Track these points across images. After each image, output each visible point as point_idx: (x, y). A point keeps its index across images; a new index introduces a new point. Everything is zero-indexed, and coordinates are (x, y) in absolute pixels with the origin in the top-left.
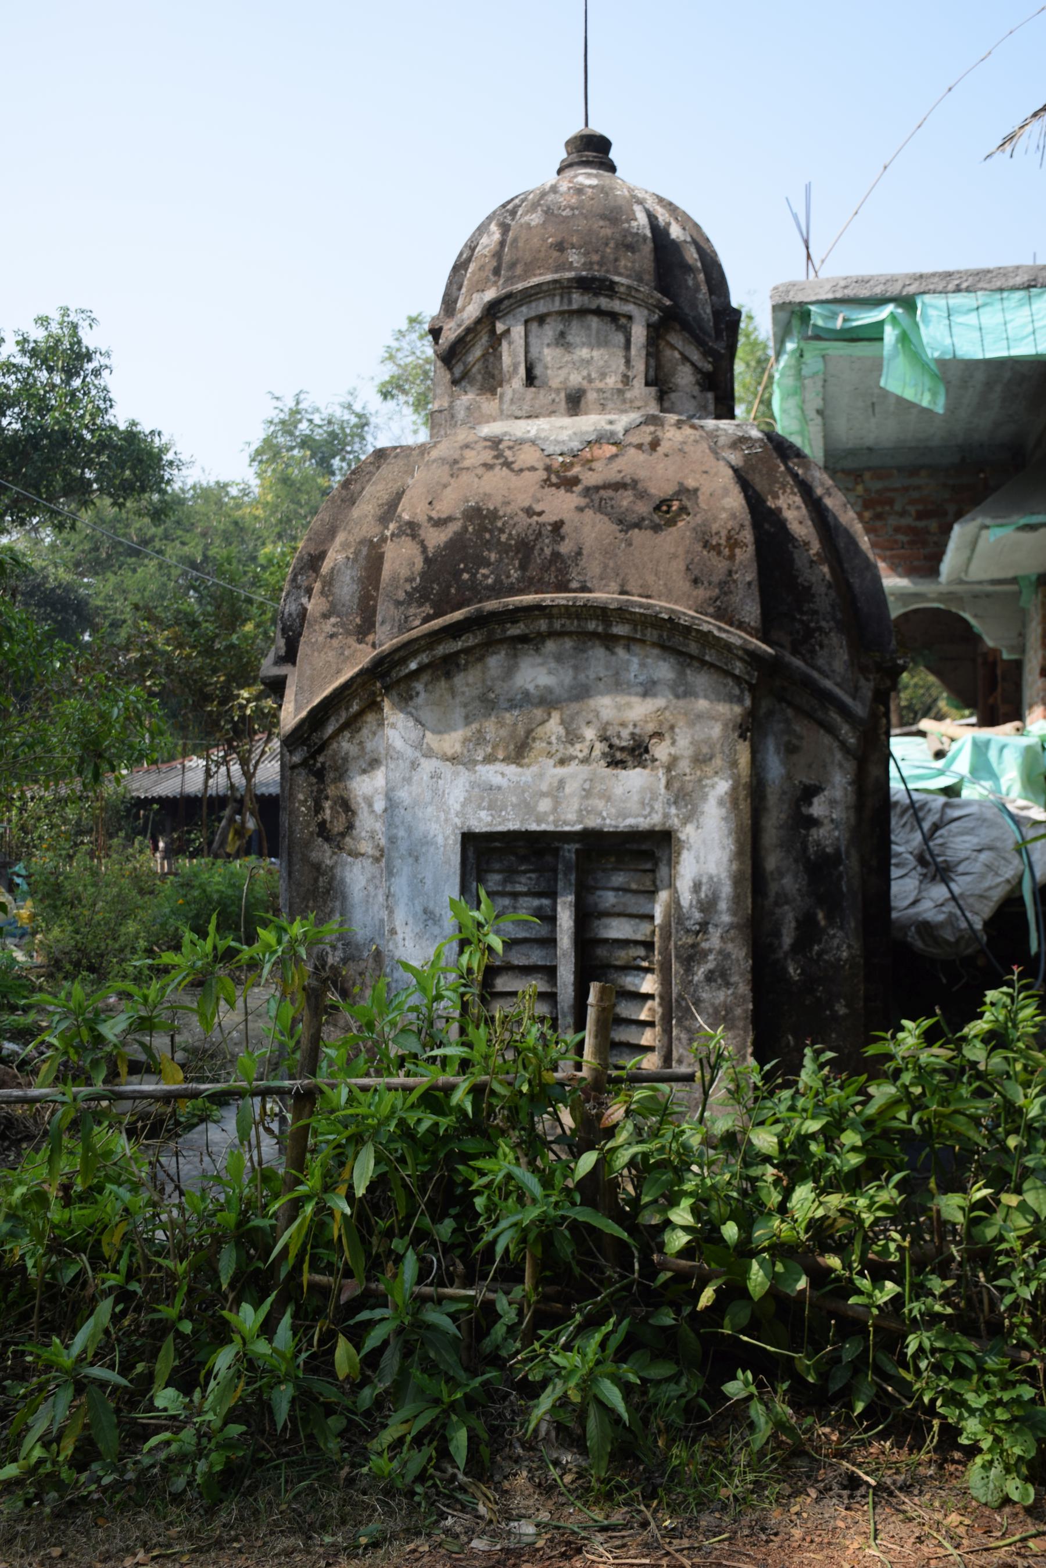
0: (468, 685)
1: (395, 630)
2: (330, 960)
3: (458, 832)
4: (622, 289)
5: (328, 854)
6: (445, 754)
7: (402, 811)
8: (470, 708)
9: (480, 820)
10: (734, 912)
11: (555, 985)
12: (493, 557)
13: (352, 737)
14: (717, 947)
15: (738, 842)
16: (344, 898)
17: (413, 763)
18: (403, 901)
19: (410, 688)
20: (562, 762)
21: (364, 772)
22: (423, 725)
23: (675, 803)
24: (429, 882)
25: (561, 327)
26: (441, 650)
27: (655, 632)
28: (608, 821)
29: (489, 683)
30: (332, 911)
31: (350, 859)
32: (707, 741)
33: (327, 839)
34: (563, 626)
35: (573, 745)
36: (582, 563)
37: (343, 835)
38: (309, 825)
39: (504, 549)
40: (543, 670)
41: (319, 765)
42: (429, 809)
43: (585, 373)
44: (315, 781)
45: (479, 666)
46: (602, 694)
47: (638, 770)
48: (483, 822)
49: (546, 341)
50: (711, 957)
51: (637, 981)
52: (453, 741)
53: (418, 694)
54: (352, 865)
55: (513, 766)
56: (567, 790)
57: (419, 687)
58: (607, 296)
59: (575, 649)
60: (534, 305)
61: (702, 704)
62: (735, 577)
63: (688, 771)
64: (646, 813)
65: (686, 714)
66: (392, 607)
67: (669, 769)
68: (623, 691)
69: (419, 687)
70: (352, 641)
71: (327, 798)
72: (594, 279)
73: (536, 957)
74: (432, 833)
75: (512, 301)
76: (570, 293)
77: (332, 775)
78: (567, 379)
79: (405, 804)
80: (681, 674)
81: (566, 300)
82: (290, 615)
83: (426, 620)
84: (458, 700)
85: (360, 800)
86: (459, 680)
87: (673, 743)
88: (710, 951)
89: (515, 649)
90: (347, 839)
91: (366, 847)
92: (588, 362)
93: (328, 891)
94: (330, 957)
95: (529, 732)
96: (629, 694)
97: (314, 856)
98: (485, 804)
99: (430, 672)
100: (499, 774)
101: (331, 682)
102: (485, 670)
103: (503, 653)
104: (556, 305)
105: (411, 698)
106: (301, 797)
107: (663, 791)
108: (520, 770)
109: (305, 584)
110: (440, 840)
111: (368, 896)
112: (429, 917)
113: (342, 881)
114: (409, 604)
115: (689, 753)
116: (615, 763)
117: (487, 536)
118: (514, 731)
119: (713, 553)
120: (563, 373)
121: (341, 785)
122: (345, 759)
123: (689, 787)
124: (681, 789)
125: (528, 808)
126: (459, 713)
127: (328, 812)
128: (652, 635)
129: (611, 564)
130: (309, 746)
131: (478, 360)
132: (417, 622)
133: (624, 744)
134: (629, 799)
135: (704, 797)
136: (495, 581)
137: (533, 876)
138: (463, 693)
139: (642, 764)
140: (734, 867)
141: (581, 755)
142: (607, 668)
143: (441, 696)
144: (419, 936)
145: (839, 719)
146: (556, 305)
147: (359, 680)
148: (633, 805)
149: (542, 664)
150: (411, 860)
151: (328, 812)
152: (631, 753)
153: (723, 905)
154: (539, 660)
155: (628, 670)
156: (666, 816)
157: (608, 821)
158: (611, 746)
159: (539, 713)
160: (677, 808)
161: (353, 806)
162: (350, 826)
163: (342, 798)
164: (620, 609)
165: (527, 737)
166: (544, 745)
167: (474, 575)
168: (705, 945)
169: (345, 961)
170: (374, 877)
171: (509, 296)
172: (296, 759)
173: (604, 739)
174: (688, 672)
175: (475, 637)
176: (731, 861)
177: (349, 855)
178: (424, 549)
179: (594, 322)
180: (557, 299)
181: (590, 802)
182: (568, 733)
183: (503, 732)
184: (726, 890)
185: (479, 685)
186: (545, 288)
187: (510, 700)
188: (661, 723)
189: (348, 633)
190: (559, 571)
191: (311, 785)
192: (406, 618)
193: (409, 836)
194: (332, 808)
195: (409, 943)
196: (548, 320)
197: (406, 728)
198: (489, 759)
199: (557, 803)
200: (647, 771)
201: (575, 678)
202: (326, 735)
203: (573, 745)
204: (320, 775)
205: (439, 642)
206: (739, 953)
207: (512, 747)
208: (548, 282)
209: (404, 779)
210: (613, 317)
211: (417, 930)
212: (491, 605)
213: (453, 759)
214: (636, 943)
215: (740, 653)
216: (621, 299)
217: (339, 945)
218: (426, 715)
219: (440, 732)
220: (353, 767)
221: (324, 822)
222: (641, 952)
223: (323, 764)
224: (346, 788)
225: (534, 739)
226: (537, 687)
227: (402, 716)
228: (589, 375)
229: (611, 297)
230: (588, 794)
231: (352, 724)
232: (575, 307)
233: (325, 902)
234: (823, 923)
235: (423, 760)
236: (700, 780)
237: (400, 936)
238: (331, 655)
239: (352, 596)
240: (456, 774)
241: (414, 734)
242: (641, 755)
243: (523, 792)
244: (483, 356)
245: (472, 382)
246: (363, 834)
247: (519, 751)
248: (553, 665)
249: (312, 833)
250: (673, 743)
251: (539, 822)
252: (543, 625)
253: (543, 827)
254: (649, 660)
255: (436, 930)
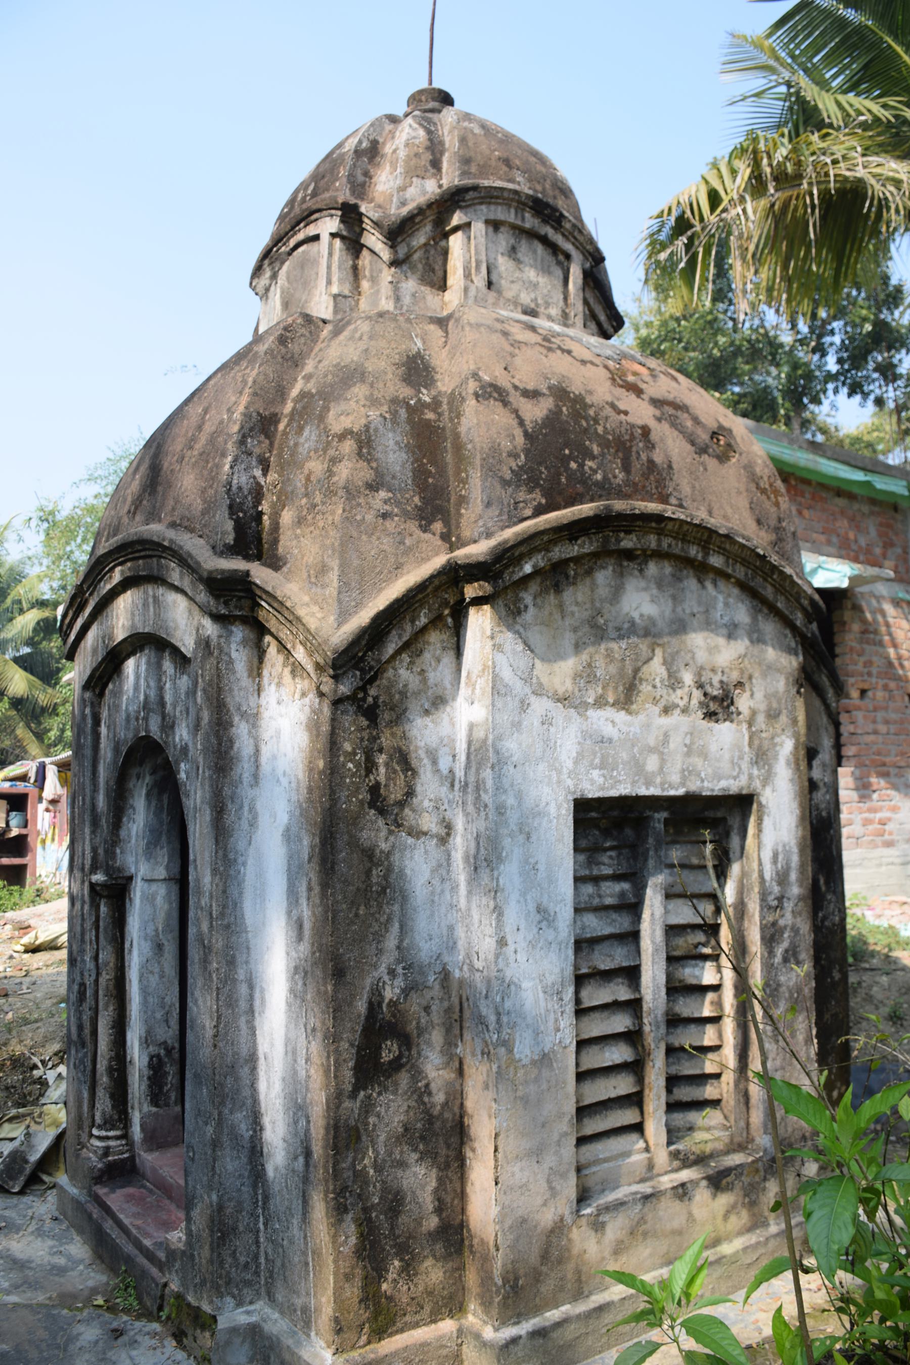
0: (577, 604)
1: (505, 517)
2: (389, 994)
3: (571, 798)
4: (568, 226)
5: (383, 834)
6: (556, 693)
7: (511, 768)
8: (580, 634)
9: (592, 782)
10: (801, 882)
11: (639, 992)
12: (596, 449)
13: (412, 663)
14: (790, 922)
15: (801, 805)
16: (405, 898)
17: (522, 702)
18: (514, 897)
19: (519, 600)
20: (666, 710)
21: (427, 712)
22: (532, 651)
23: (756, 762)
24: (541, 867)
25: (512, 241)
26: (559, 552)
27: (743, 569)
28: (706, 784)
29: (598, 605)
30: (389, 920)
31: (410, 840)
32: (775, 694)
33: (382, 812)
34: (670, 546)
35: (674, 690)
36: (675, 478)
37: (401, 804)
38: (357, 790)
39: (605, 444)
40: (645, 597)
41: (370, 700)
42: (541, 767)
43: (533, 296)
44: (365, 723)
45: (588, 581)
46: (695, 631)
47: (727, 723)
48: (597, 785)
49: (501, 250)
50: (786, 935)
51: (697, 972)
52: (562, 673)
53: (526, 607)
54: (413, 848)
55: (623, 713)
56: (672, 746)
57: (528, 598)
58: (552, 227)
59: (673, 576)
60: (493, 207)
61: (771, 653)
62: (784, 524)
63: (763, 727)
64: (735, 774)
65: (760, 664)
66: (498, 487)
67: (750, 724)
68: (712, 631)
69: (528, 598)
70: (412, 526)
71: (381, 750)
72: (547, 205)
73: (618, 957)
74: (544, 800)
75: (476, 194)
76: (523, 210)
77: (387, 716)
78: (518, 295)
79: (515, 759)
80: (754, 619)
81: (519, 215)
82: (240, 488)
83: (539, 511)
84: (568, 621)
85: (422, 753)
86: (568, 595)
87: (752, 695)
88: (785, 927)
89: (621, 565)
90: (407, 811)
91: (429, 822)
92: (536, 286)
93: (384, 891)
94: (388, 988)
95: (636, 671)
96: (717, 635)
97: (365, 836)
98: (597, 761)
99: (538, 580)
100: (609, 721)
101: (389, 581)
102: (594, 587)
103: (611, 568)
104: (511, 217)
105: (519, 613)
106: (347, 747)
107: (747, 749)
108: (629, 718)
109: (257, 451)
110: (552, 810)
111: (433, 893)
112: (544, 915)
113: (402, 874)
114: (518, 486)
115: (762, 707)
116: (710, 715)
117: (584, 424)
118: (622, 669)
119: (764, 497)
120: (516, 287)
121: (398, 731)
122: (403, 694)
123: (766, 744)
124: (760, 747)
125: (638, 767)
126: (569, 639)
127: (382, 770)
128: (740, 572)
129: (697, 485)
130: (362, 670)
131: (420, 248)
132: (528, 512)
133: (715, 693)
134: (712, 758)
135: (776, 757)
136: (605, 478)
137: (613, 853)
138: (573, 614)
139: (729, 718)
140: (800, 833)
141: (682, 703)
142: (699, 603)
143: (551, 614)
144: (532, 945)
145: (827, 683)
146: (511, 217)
147: (436, 582)
148: (725, 766)
149: (645, 589)
150: (521, 838)
151: (382, 770)
152: (719, 705)
153: (793, 876)
154: (643, 584)
155: (715, 608)
156: (751, 777)
157: (706, 784)
158: (705, 695)
159: (643, 647)
160: (759, 770)
161: (414, 763)
162: (410, 793)
163: (400, 750)
164: (727, 536)
165: (634, 678)
166: (650, 688)
167: (581, 466)
168: (782, 922)
169: (406, 992)
170: (440, 866)
171: (475, 188)
172: (344, 689)
173: (700, 686)
174: (760, 618)
175: (591, 543)
176: (797, 827)
177: (409, 834)
178: (521, 423)
179: (540, 248)
180: (513, 211)
181: (691, 760)
182: (670, 676)
183: (613, 669)
184: (795, 859)
185: (588, 606)
186: (506, 194)
187: (618, 629)
188: (742, 672)
189: (406, 515)
190: (657, 479)
191: (361, 729)
192: (516, 503)
193: (520, 804)
194: (387, 765)
195: (522, 957)
196: (502, 229)
197: (514, 652)
198: (600, 703)
199: (663, 761)
200: (734, 726)
201: (674, 611)
202: (386, 656)
203: (674, 690)
204: (371, 714)
205: (554, 542)
206: (805, 927)
207: (621, 688)
208: (510, 190)
209: (513, 725)
210: (554, 248)
211: (530, 937)
212: (619, 505)
213: (563, 700)
214: (694, 927)
215: (806, 603)
216: (564, 235)
217: (400, 970)
218: (536, 637)
219: (549, 661)
220: (414, 707)
221: (377, 785)
222: (701, 937)
223: (376, 698)
224: (404, 737)
225: (641, 680)
226: (641, 615)
227: (509, 635)
228: (536, 299)
229: (555, 229)
230: (689, 751)
231: (412, 646)
232: (527, 225)
233: (380, 906)
234: (823, 888)
235: (533, 699)
236: (773, 738)
237: (511, 948)
238: (387, 543)
239: (403, 466)
240: (568, 719)
241: (523, 660)
242: (728, 707)
243: (633, 746)
244: (425, 245)
245: (413, 268)
246: (426, 804)
247: (627, 695)
248: (655, 591)
249: (361, 802)
250: (752, 695)
251: (648, 785)
252: (652, 541)
253: (653, 791)
254: (731, 600)
255: (550, 935)
